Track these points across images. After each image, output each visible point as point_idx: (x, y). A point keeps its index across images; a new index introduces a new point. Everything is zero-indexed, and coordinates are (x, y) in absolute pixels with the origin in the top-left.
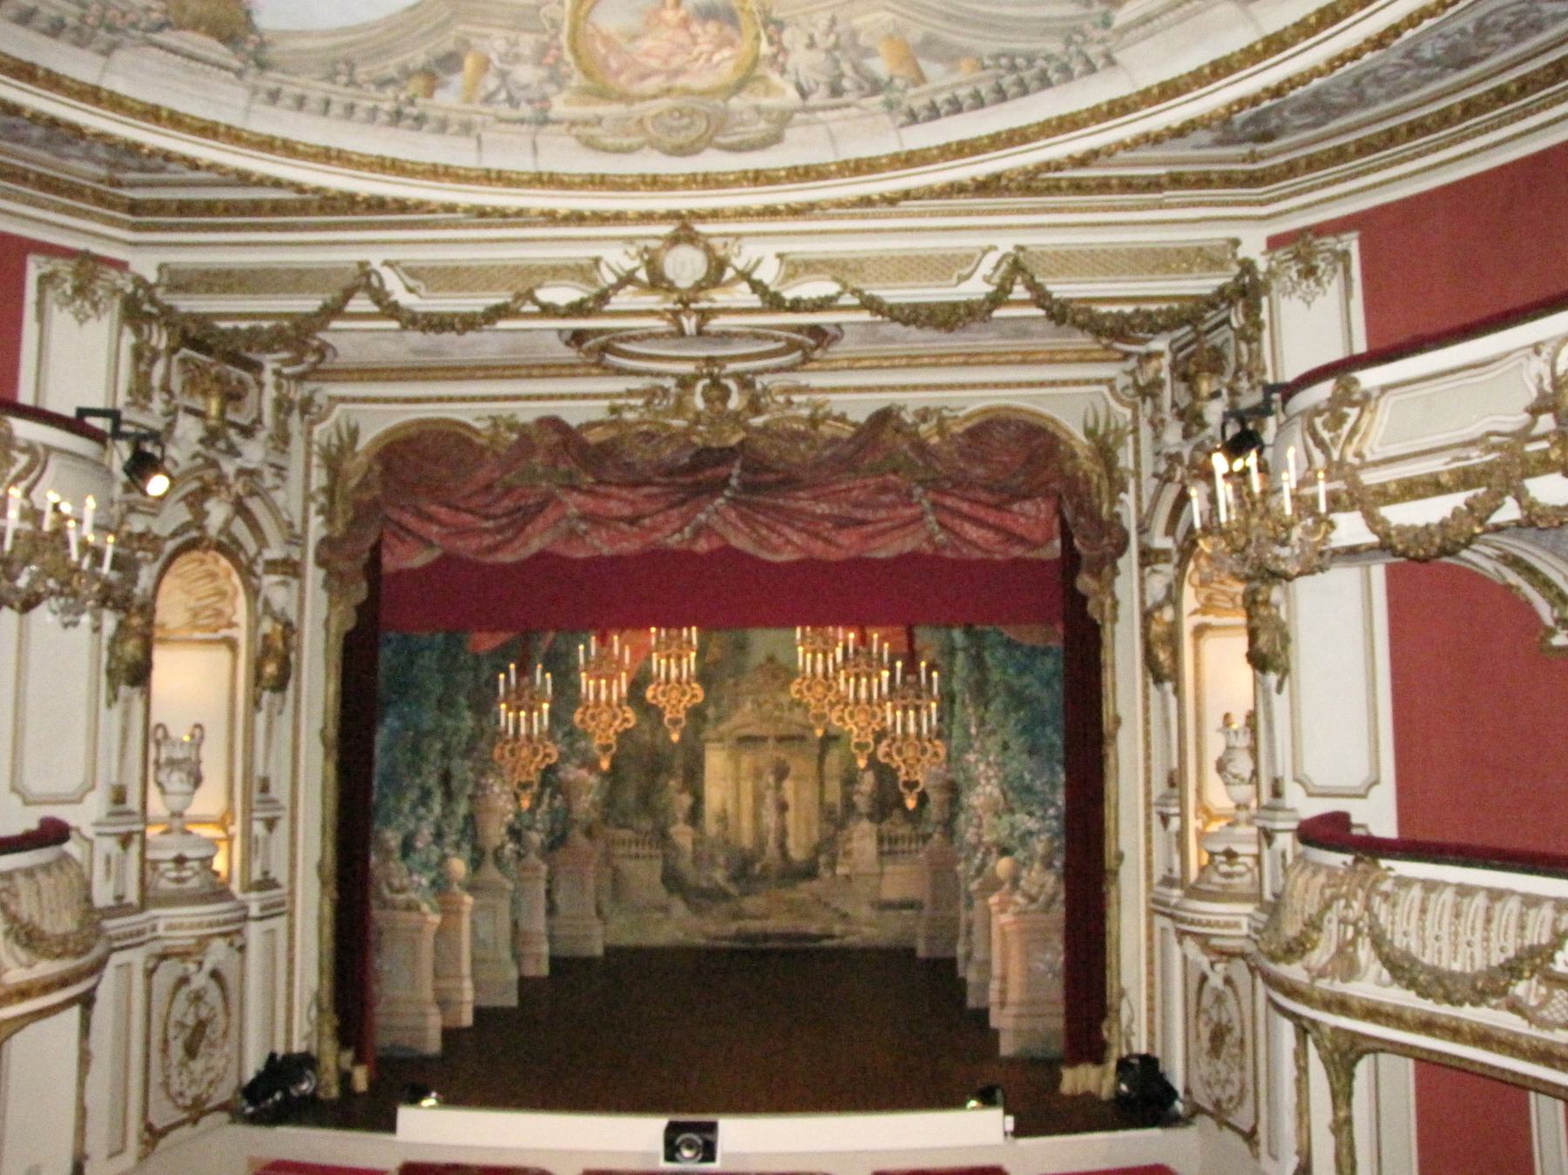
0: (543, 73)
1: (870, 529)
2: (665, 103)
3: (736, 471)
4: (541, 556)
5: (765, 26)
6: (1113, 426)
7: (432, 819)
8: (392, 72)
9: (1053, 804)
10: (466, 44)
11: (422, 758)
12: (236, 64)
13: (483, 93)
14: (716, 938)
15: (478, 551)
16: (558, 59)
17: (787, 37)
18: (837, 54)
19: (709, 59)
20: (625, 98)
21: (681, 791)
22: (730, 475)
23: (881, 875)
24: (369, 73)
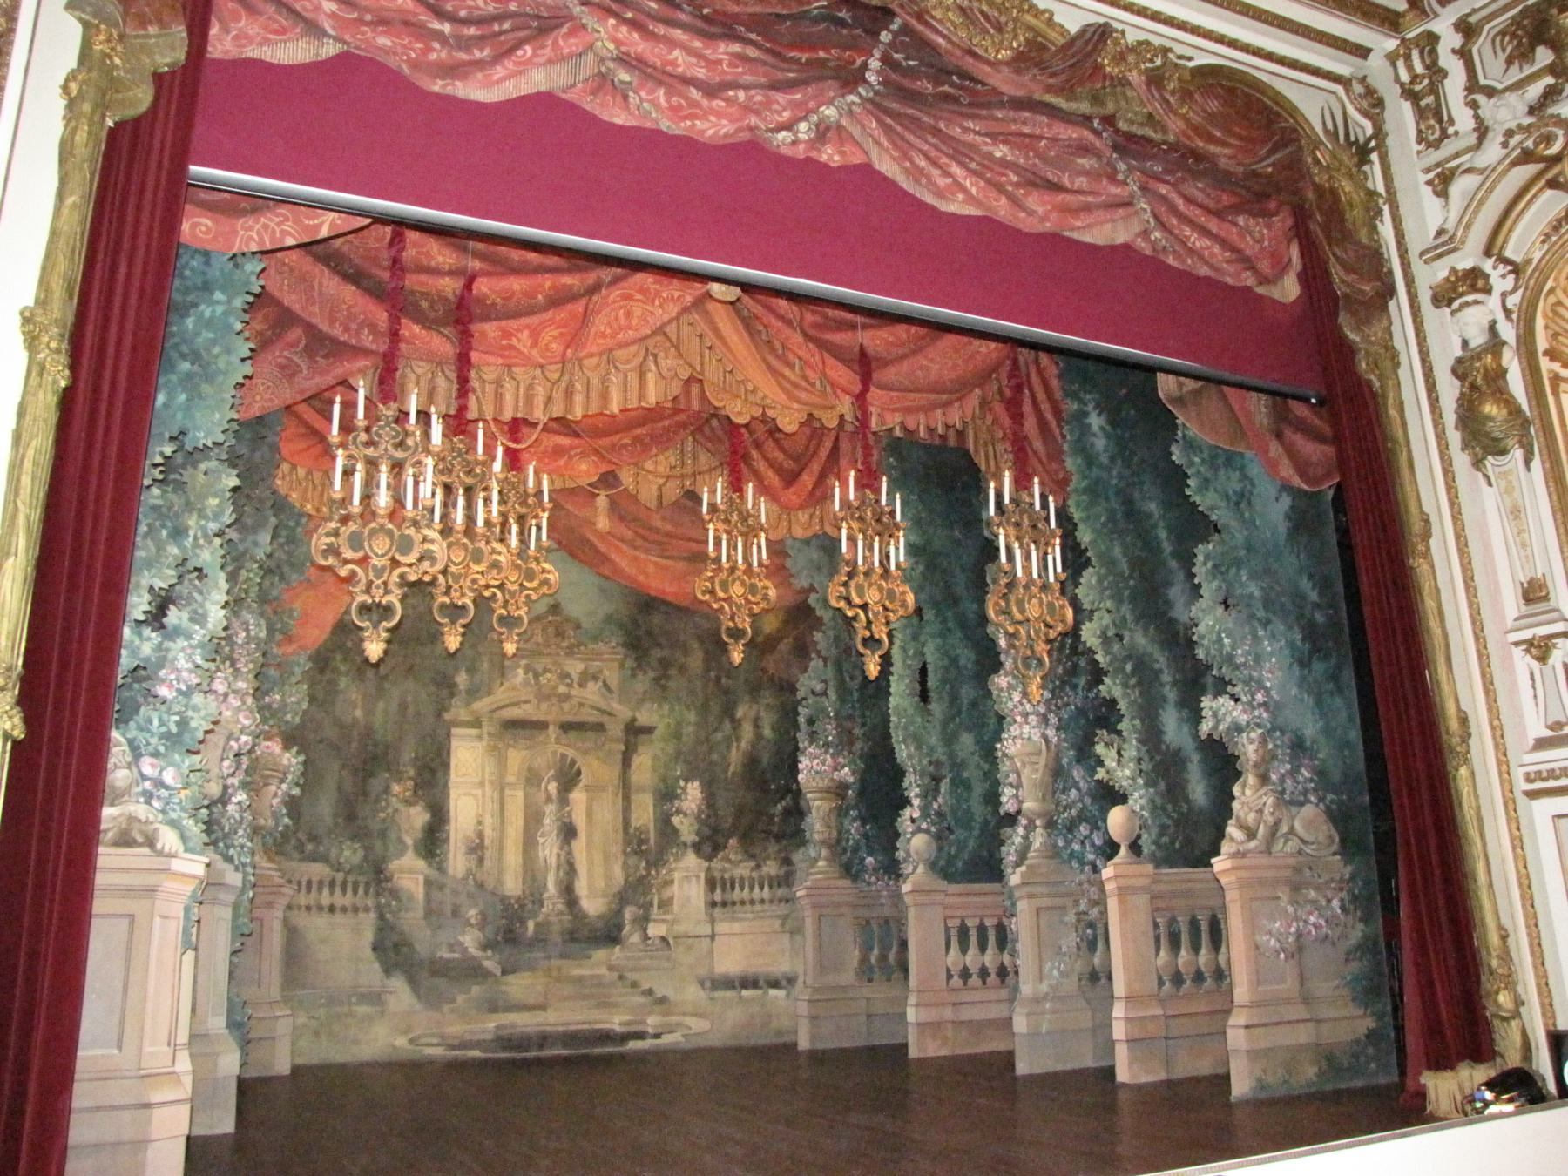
1: (1069, 198)
3: (875, 64)
4: (544, 102)
6: (1353, 139)
7: (199, 634)
9: (1261, 686)
11: (189, 507)
14: (464, 1045)
15: (415, 65)
21: (407, 802)
22: (865, 66)
23: (713, 937)
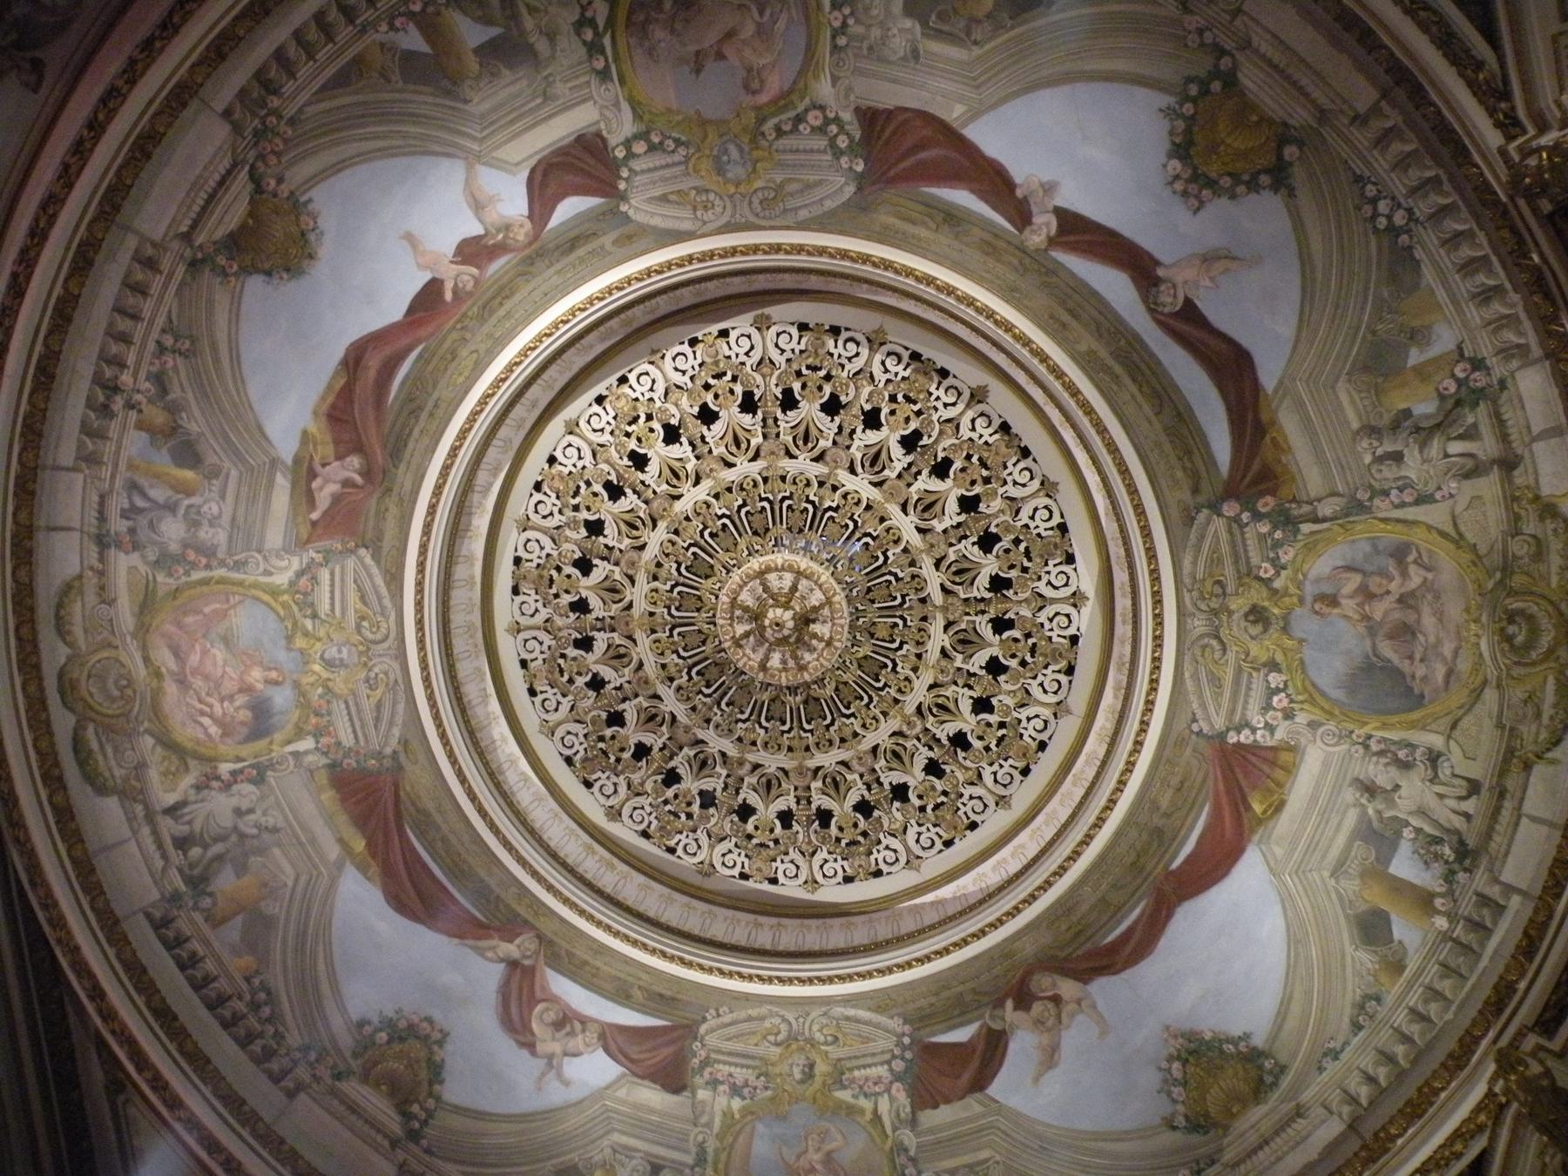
0: (174, 547)
5: (252, 766)
8: (175, 394)
10: (214, 473)
12: (200, 239)
13: (143, 482)
16: (194, 566)
17: (248, 788)
18: (234, 838)
19: (203, 713)
24: (175, 368)
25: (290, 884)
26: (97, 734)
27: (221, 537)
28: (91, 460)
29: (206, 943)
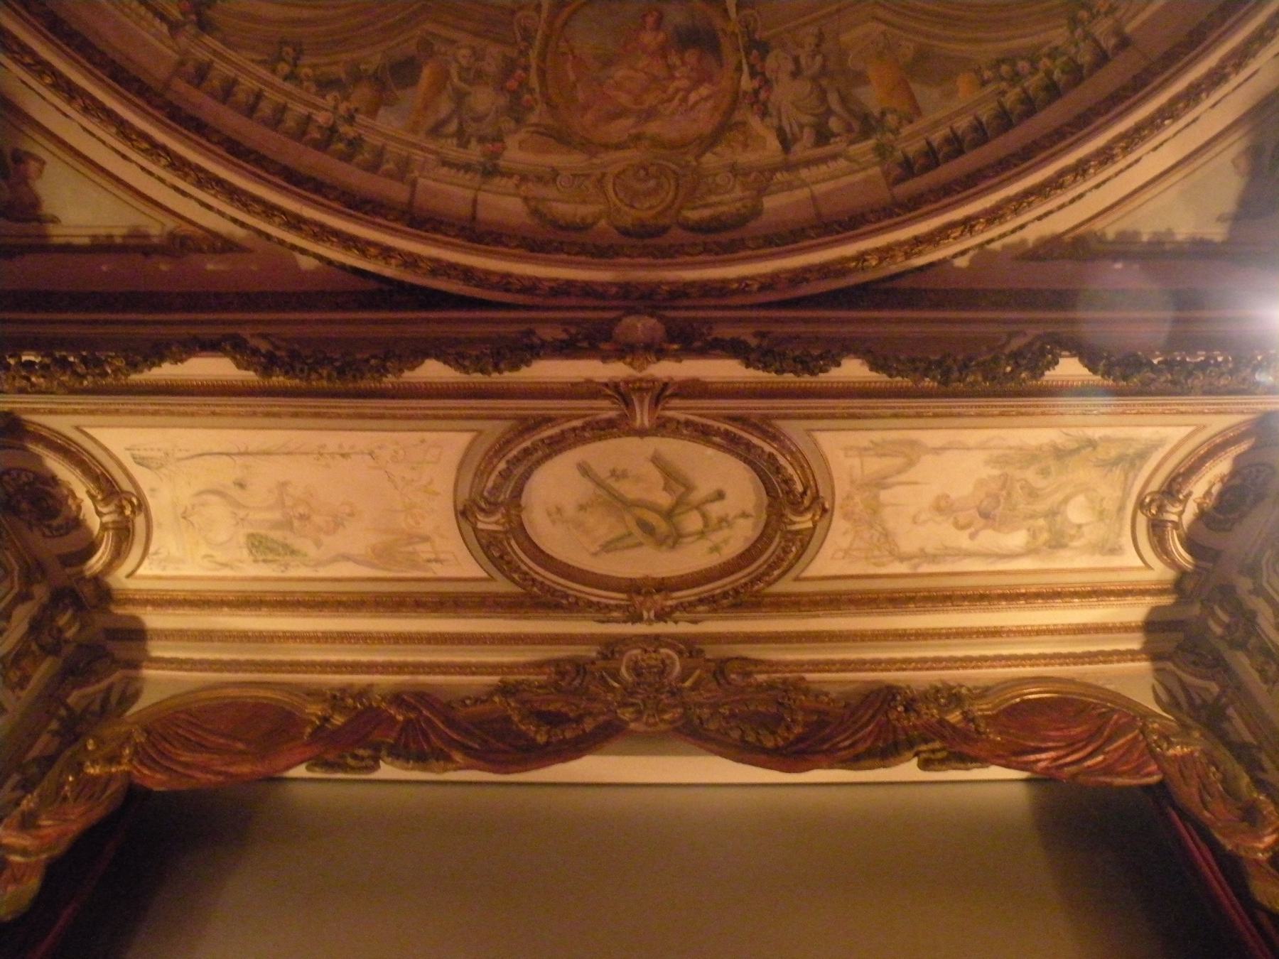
0: (503, 101)
2: (632, 155)
5: (748, 54)
8: (340, 72)
10: (426, 46)
12: (175, 13)
16: (523, 84)
17: (771, 62)
18: (824, 82)
19: (684, 100)
20: (588, 146)
24: (313, 67)
25: (883, 27)
26: (694, 208)
27: (494, 50)
28: (403, 171)
29: (936, 124)
